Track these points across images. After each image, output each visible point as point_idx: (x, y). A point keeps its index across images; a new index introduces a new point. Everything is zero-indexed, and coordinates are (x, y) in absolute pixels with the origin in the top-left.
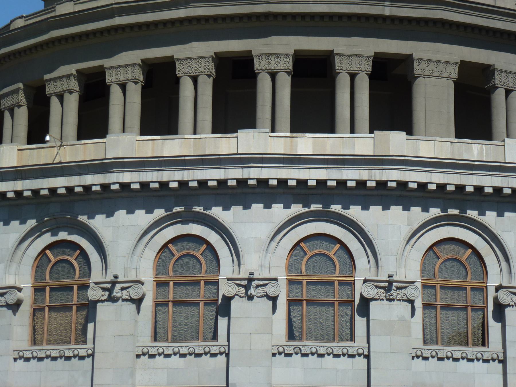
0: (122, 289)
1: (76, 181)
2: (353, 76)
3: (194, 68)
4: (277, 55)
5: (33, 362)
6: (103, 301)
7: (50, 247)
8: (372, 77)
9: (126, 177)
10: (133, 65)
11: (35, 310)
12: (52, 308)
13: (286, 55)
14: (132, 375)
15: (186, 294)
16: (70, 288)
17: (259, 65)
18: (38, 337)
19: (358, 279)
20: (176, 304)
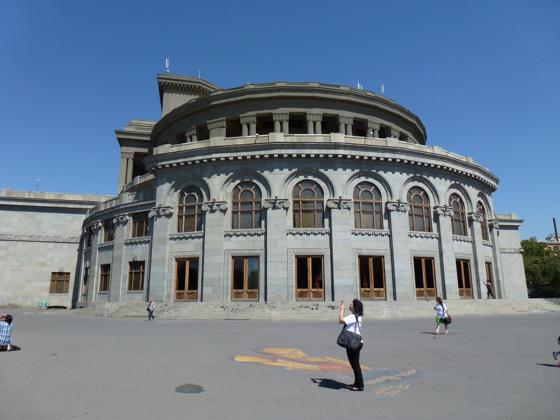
0: (402, 206)
1: (382, 155)
3: (346, 121)
4: (376, 123)
5: (360, 236)
6: (393, 211)
7: (360, 184)
9: (403, 157)
10: (320, 115)
11: (355, 212)
12: (364, 212)
13: (378, 124)
14: (408, 244)
15: (419, 212)
16: (371, 204)
17: (370, 125)
18: (358, 225)
19: (467, 212)
20: (415, 215)
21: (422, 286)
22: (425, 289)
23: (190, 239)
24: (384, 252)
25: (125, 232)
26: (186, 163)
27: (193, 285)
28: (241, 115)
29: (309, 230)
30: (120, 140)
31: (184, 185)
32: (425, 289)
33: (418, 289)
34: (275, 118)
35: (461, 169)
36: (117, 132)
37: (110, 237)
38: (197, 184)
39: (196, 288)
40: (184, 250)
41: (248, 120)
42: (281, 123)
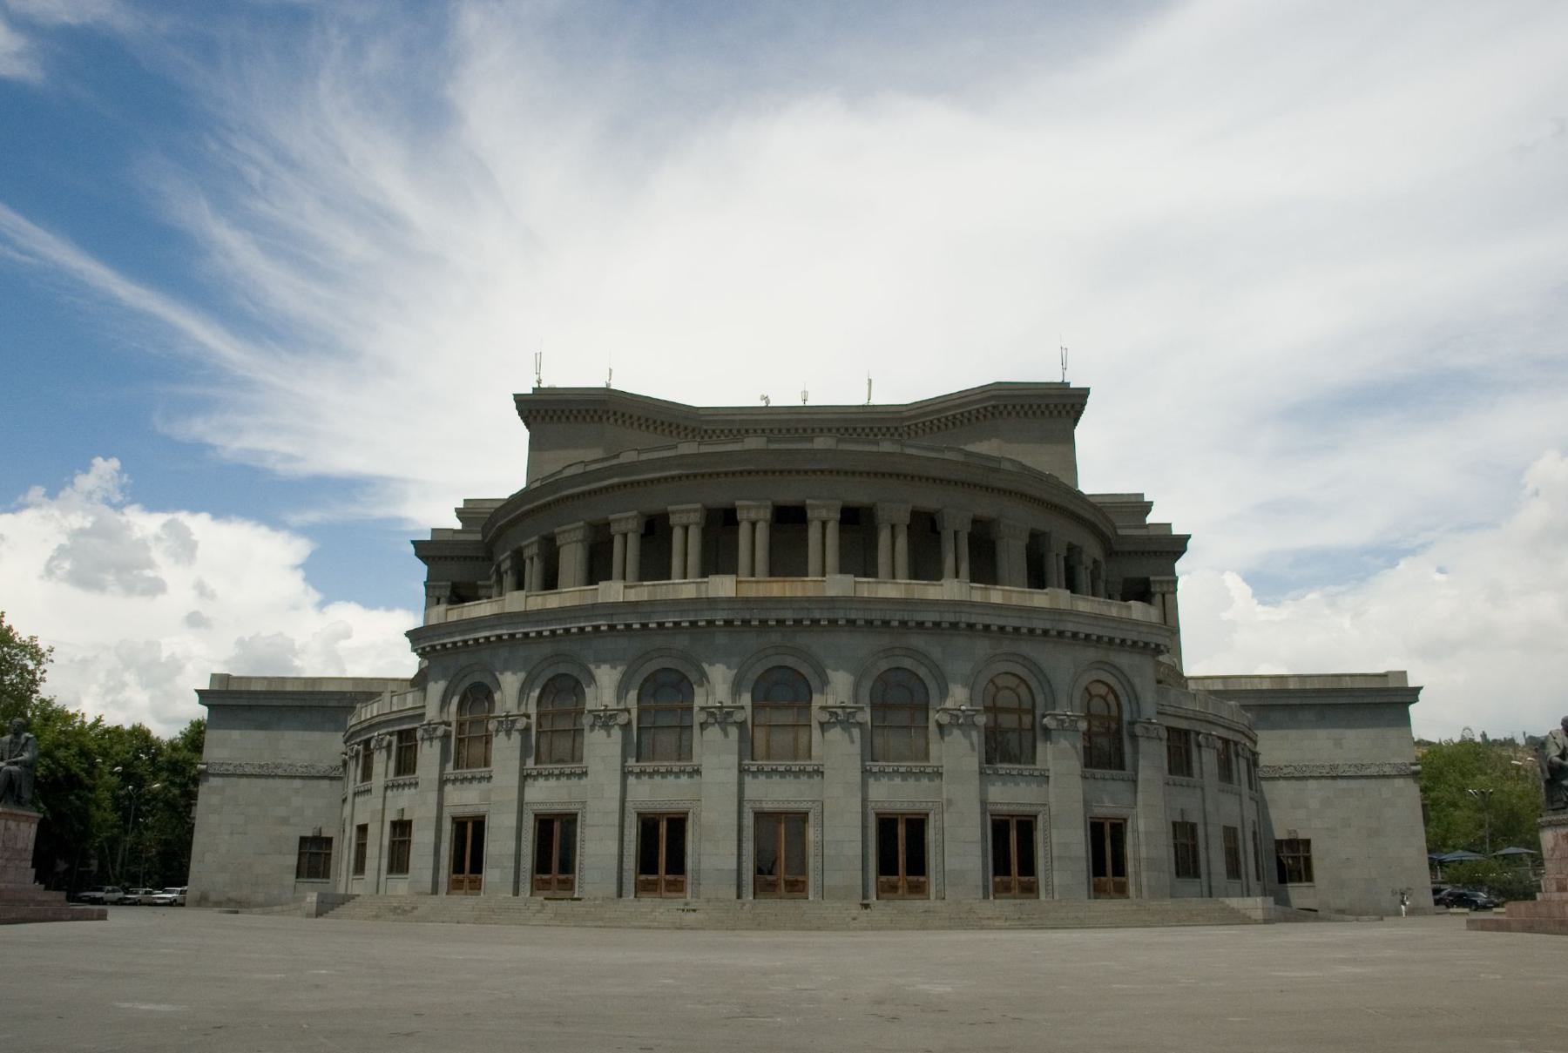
2: (956, 533)
7: (767, 671)
8: (971, 536)
19: (1038, 712)
21: (896, 873)
22: (901, 879)
23: (475, 783)
24: (809, 805)
25: (382, 765)
26: (465, 642)
27: (477, 867)
28: (612, 517)
29: (663, 765)
30: (421, 558)
31: (467, 683)
32: (901, 879)
33: (883, 879)
34: (673, 520)
35: (1011, 622)
36: (413, 542)
37: (367, 775)
38: (487, 681)
39: (480, 872)
40: (464, 802)
41: (623, 527)
42: (686, 529)
